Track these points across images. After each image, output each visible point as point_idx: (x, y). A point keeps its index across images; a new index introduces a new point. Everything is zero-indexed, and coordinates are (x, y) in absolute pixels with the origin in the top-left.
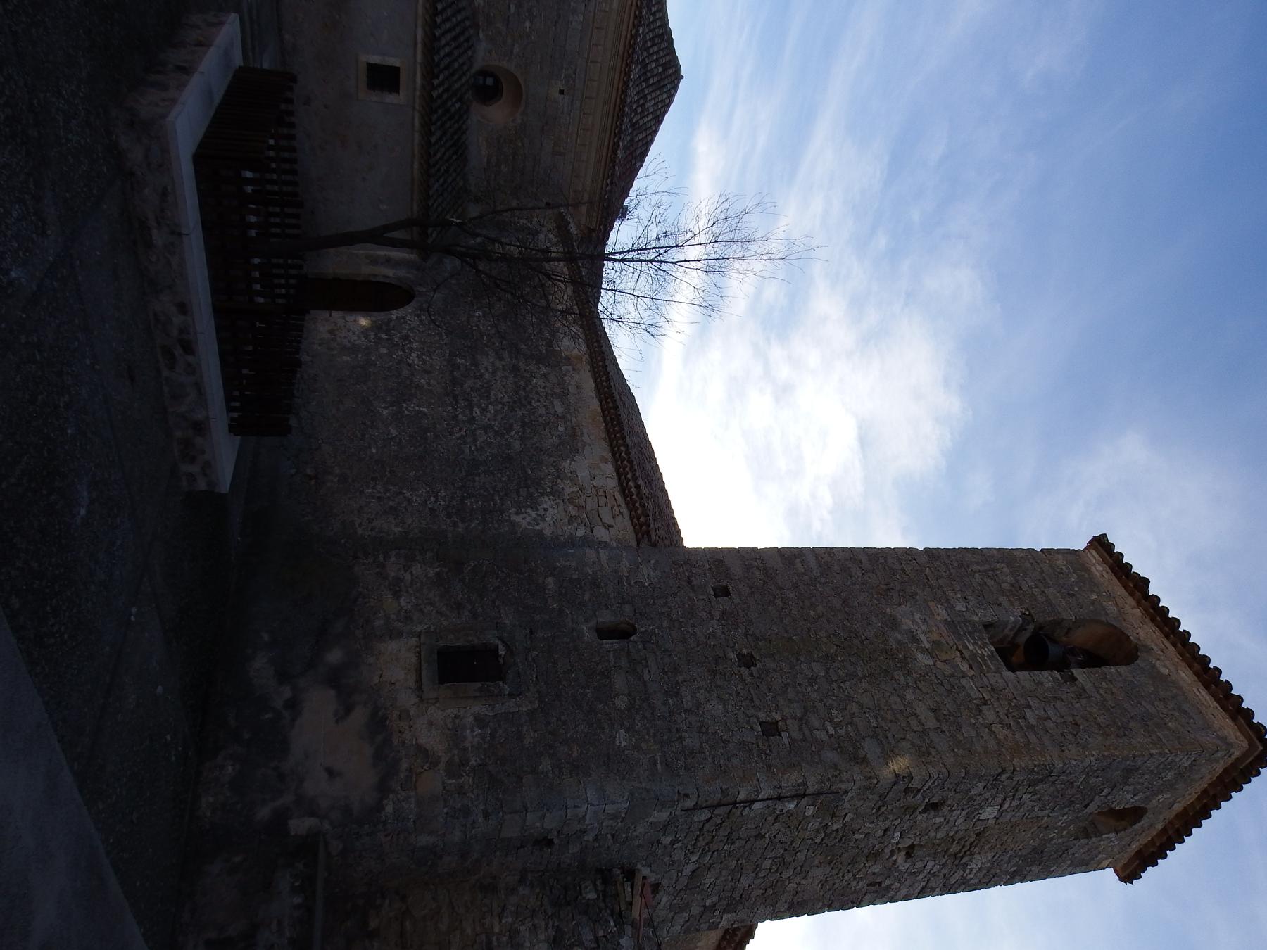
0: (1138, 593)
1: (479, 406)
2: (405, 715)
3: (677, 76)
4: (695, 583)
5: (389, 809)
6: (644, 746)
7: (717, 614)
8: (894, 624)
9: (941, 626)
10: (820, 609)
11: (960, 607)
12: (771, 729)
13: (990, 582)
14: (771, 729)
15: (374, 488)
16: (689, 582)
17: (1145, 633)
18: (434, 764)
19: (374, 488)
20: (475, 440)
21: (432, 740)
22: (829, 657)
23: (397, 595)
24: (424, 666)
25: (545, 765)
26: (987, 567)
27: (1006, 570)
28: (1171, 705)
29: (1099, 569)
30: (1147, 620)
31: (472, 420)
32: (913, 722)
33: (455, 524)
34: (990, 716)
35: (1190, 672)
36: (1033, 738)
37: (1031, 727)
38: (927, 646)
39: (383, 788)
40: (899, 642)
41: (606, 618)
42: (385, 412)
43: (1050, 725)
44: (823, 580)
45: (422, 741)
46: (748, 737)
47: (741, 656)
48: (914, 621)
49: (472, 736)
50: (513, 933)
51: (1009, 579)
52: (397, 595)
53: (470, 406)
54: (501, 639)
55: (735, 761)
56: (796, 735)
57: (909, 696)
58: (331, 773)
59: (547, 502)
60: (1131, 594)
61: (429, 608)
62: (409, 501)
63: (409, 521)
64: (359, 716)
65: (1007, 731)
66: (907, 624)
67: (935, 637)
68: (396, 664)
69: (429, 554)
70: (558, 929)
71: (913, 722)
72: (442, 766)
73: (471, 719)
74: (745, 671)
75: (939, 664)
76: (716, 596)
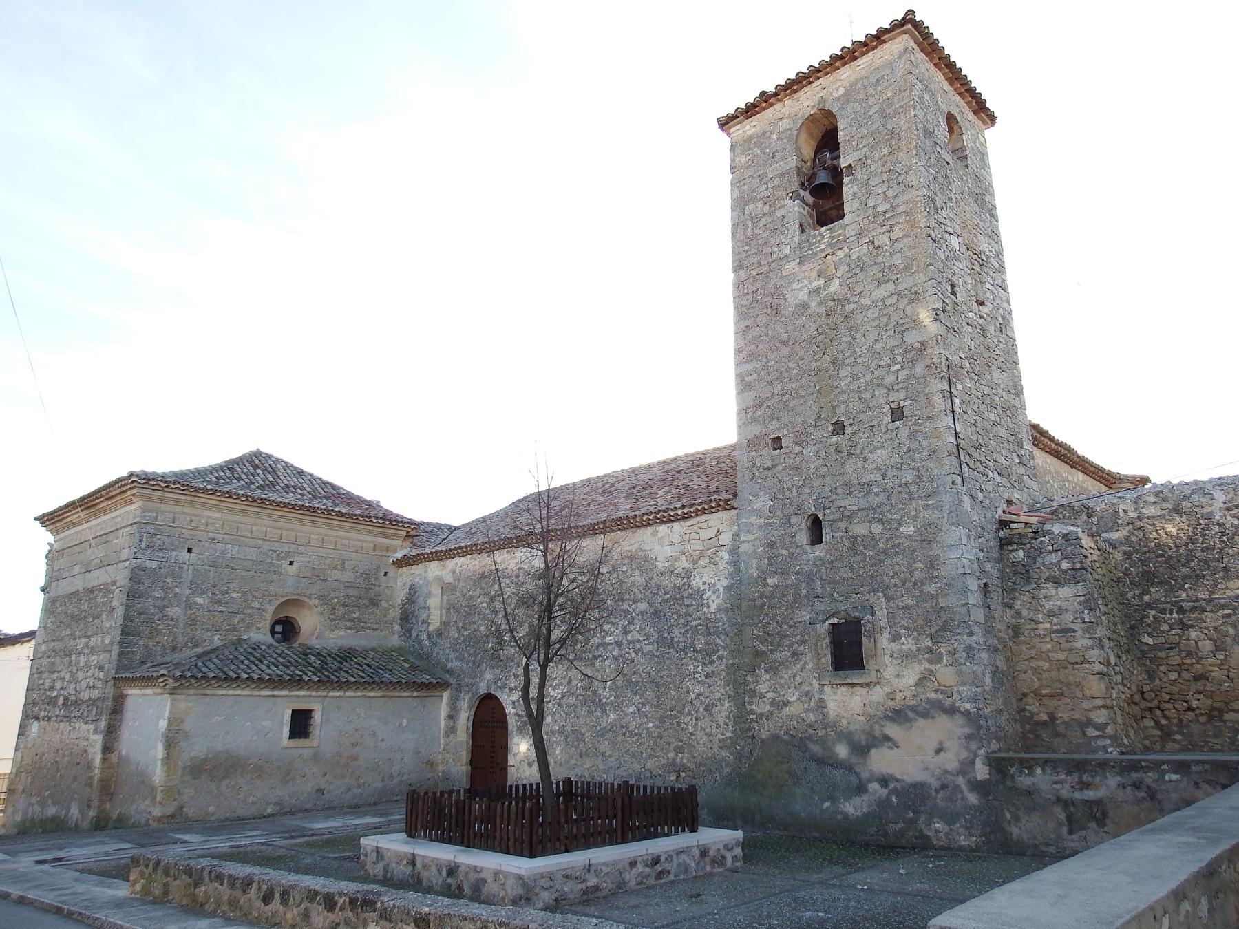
0: (772, 100)
1: (604, 637)
2: (891, 696)
3: (258, 454)
4: (769, 465)
5: (967, 706)
6: (913, 513)
7: (798, 449)
8: (804, 307)
9: (804, 268)
10: (791, 365)
11: (786, 250)
12: (897, 414)
13: (763, 222)
14: (897, 414)
15: (687, 724)
17: (806, 102)
18: (931, 673)
19: (687, 724)
20: (639, 641)
21: (911, 675)
23: (786, 704)
24: (849, 681)
25: (930, 589)
26: (749, 222)
27: (751, 206)
28: (871, 91)
29: (749, 128)
30: (795, 96)
31: (618, 644)
32: (889, 301)
33: (720, 658)
34: (882, 240)
35: (842, 70)
36: (902, 209)
37: (893, 208)
38: (822, 281)
39: (951, 711)
40: (820, 304)
41: (803, 537)
42: (612, 716)
43: (890, 193)
44: (764, 360)
45: (912, 683)
46: (904, 432)
47: (834, 432)
48: (800, 289)
49: (908, 644)
50: (1051, 614)
52: (786, 704)
53: (604, 645)
54: (824, 622)
55: (925, 444)
56: (902, 394)
57: (867, 302)
58: (939, 750)
59: (697, 582)
60: (772, 105)
61: (798, 678)
62: (699, 695)
63: (718, 695)
64: (892, 730)
65: (896, 228)
66: (803, 296)
67: (814, 274)
68: (847, 703)
69: (749, 678)
70: (1047, 580)
71: (889, 301)
72: (932, 667)
73: (893, 645)
74: (848, 430)
75: (839, 274)
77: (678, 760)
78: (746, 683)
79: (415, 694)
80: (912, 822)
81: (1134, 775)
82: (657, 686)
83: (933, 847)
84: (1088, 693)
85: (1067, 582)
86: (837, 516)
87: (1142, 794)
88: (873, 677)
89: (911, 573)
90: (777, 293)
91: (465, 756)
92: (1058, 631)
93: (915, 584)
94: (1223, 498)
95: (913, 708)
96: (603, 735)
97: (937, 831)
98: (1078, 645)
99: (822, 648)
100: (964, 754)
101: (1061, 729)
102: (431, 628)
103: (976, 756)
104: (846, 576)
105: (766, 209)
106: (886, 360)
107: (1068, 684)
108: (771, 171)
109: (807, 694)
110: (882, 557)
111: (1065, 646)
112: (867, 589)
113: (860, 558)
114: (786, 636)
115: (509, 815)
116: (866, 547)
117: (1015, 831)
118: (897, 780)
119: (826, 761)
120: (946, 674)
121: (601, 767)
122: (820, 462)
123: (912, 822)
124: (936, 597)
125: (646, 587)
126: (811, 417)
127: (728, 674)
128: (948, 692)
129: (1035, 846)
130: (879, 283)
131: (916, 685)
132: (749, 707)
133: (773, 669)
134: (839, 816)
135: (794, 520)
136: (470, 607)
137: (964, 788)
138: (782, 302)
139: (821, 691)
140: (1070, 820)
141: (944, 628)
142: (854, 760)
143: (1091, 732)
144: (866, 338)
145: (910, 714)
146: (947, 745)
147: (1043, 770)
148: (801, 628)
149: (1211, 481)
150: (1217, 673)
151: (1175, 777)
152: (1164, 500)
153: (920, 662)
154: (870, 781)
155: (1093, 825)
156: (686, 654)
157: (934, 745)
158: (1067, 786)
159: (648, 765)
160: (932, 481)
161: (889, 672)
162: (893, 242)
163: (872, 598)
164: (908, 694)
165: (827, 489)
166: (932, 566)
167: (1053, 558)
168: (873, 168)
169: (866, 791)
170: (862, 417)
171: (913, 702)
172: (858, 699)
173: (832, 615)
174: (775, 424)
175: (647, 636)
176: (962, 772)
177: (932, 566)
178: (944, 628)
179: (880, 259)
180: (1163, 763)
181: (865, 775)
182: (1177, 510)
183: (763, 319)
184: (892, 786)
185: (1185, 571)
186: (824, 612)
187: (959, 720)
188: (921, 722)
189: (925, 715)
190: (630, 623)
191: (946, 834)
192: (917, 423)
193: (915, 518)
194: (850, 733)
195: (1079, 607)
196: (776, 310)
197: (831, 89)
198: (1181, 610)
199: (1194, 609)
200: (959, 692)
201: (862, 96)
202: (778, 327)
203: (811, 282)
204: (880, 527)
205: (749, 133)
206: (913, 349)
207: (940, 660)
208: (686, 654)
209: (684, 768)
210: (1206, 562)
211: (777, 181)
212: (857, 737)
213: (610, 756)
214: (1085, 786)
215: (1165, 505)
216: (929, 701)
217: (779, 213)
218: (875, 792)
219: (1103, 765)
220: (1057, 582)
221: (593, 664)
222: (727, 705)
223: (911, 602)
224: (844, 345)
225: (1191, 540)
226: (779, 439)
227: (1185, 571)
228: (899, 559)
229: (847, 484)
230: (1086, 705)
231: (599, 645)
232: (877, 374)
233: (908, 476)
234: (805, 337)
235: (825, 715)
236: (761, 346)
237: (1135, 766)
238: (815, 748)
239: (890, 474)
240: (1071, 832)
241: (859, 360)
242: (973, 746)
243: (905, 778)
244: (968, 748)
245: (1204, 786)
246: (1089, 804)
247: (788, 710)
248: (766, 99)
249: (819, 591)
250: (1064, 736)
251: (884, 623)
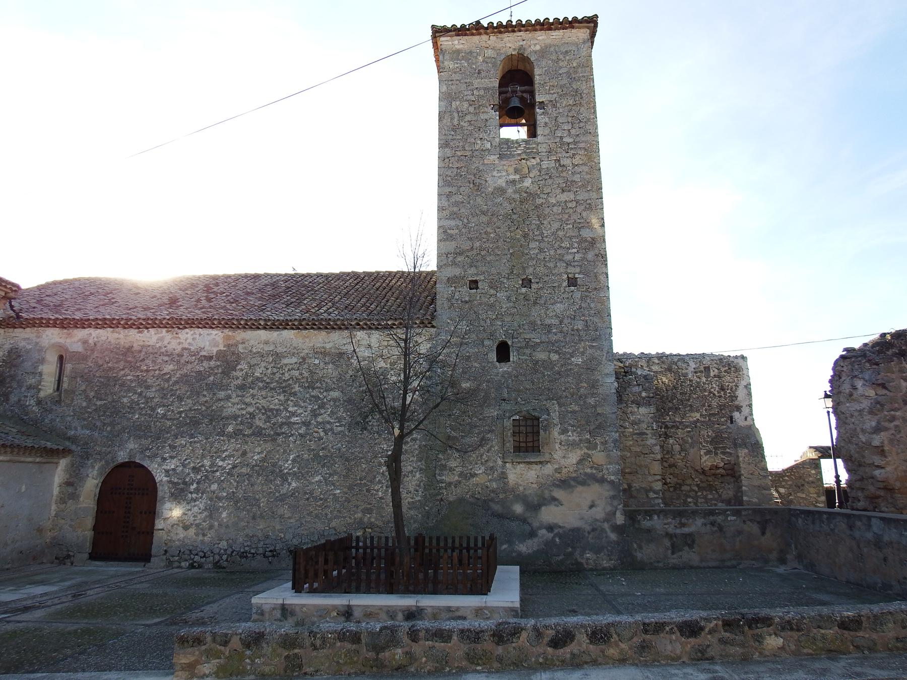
0: (482, 31)
1: (289, 417)
4: (467, 299)
5: (613, 478)
6: (582, 350)
7: (492, 292)
8: (501, 191)
9: (503, 163)
10: (489, 230)
11: (488, 146)
12: (572, 282)
13: (468, 118)
14: (572, 282)
15: (378, 491)
16: (466, 302)
17: (510, 43)
18: (589, 456)
19: (378, 491)
20: (329, 423)
21: (574, 457)
22: (525, 236)
23: (473, 475)
24: (528, 460)
25: (591, 401)
26: (456, 115)
27: (458, 103)
28: (561, 57)
29: (458, 43)
30: (500, 36)
31: (306, 424)
32: (569, 205)
33: (414, 440)
34: (566, 162)
35: (539, 33)
36: (582, 145)
37: (575, 143)
38: (518, 177)
39: (602, 481)
40: (515, 192)
41: (493, 356)
42: (294, 485)
43: (573, 132)
44: (465, 220)
45: (575, 462)
46: (577, 295)
47: (523, 286)
48: (500, 177)
49: (573, 437)
50: (634, 423)
51: (466, 105)
52: (473, 475)
53: (290, 424)
54: (509, 418)
55: (592, 305)
56: (578, 270)
57: (553, 201)
58: (591, 507)
60: (480, 34)
61: (484, 457)
64: (558, 494)
65: (578, 157)
66: (501, 182)
67: (511, 170)
68: (523, 476)
69: (440, 456)
70: (633, 402)
71: (569, 205)
72: (590, 452)
73: (562, 436)
74: (534, 286)
75: (532, 175)
76: (477, 288)
77: (366, 520)
78: (437, 460)
79: (38, 460)
80: (571, 554)
81: (712, 518)
82: (347, 460)
83: (585, 569)
84: (652, 472)
85: (644, 405)
86: (523, 344)
87: (716, 529)
88: (547, 457)
89: (578, 389)
90: (478, 173)
91: (90, 522)
92: (637, 434)
93: (581, 397)
94: (694, 366)
95: (574, 479)
96: (282, 500)
97: (588, 559)
98: (649, 443)
99: (507, 436)
100: (609, 509)
101: (635, 493)
102: (42, 394)
103: (617, 509)
104: (528, 387)
105: (471, 109)
106: (566, 244)
107: (640, 466)
108: (476, 83)
109: (492, 468)
110: (557, 376)
111: (640, 443)
112: (544, 397)
113: (540, 375)
114: (476, 426)
115: (123, 575)
116: (545, 368)
117: (639, 555)
118: (560, 527)
119: (506, 516)
120: (599, 457)
121: (278, 527)
122: (511, 304)
123: (571, 554)
124: (595, 407)
125: (340, 379)
126: (505, 271)
127: (420, 453)
128: (599, 468)
129: (651, 563)
130: (563, 191)
131: (578, 463)
132: (439, 478)
133: (464, 452)
134: (514, 554)
135: (487, 342)
136: (108, 378)
137: (608, 530)
138: (484, 183)
139: (504, 467)
140: (673, 546)
141: (599, 427)
142: (528, 514)
143: (652, 495)
144: (550, 227)
145: (572, 483)
146: (598, 502)
147: (658, 517)
148: (489, 422)
149: (687, 355)
150: (680, 464)
151: (733, 518)
152: (663, 362)
153: (581, 449)
154: (540, 528)
155: (686, 548)
156: (380, 435)
157: (588, 503)
158: (672, 526)
159: (333, 524)
160: (596, 330)
161: (558, 455)
162: (574, 166)
163: (548, 404)
164: (571, 469)
165: (516, 324)
166: (593, 386)
167: (636, 389)
168: (561, 110)
169: (536, 536)
170: (546, 279)
171: (574, 475)
172: (533, 472)
173: (516, 414)
174: (473, 270)
175: (339, 420)
176: (606, 520)
177: (593, 386)
178: (599, 427)
179: (564, 174)
180: (728, 510)
181: (536, 524)
182: (669, 369)
183: (466, 190)
184: (556, 531)
185: (670, 405)
186: (510, 411)
187: (607, 486)
188: (580, 488)
189: (583, 483)
190: (320, 407)
191: (594, 561)
192: (587, 291)
193: (583, 353)
194: (525, 496)
195: (651, 420)
196: (478, 187)
197: (536, 42)
198: (666, 427)
199: (673, 427)
200: (607, 469)
201: (554, 58)
202: (479, 200)
203: (508, 175)
204: (557, 357)
205: (458, 47)
206: (586, 241)
207: (595, 448)
208: (380, 435)
209: (372, 526)
210: (682, 401)
211: (482, 92)
212: (530, 499)
213: (289, 518)
214: (683, 525)
215: (663, 366)
216: (586, 474)
217: (483, 116)
218: (543, 536)
219: (694, 513)
220: (639, 405)
221: (274, 440)
222: (418, 475)
223: (577, 408)
224: (533, 226)
225: (675, 388)
226: (476, 282)
227: (670, 405)
228: (570, 379)
229: (533, 324)
230: (650, 479)
231: (283, 424)
232: (559, 252)
233: (580, 325)
234: (502, 212)
235: (506, 484)
236: (463, 210)
237: (712, 513)
238: (496, 507)
239: (566, 321)
240: (673, 553)
241: (546, 240)
242: (615, 503)
243: (566, 525)
244: (611, 505)
245: (748, 523)
246: (685, 536)
247: (475, 480)
248: (477, 28)
249: (506, 395)
250: (635, 497)
251: (556, 421)
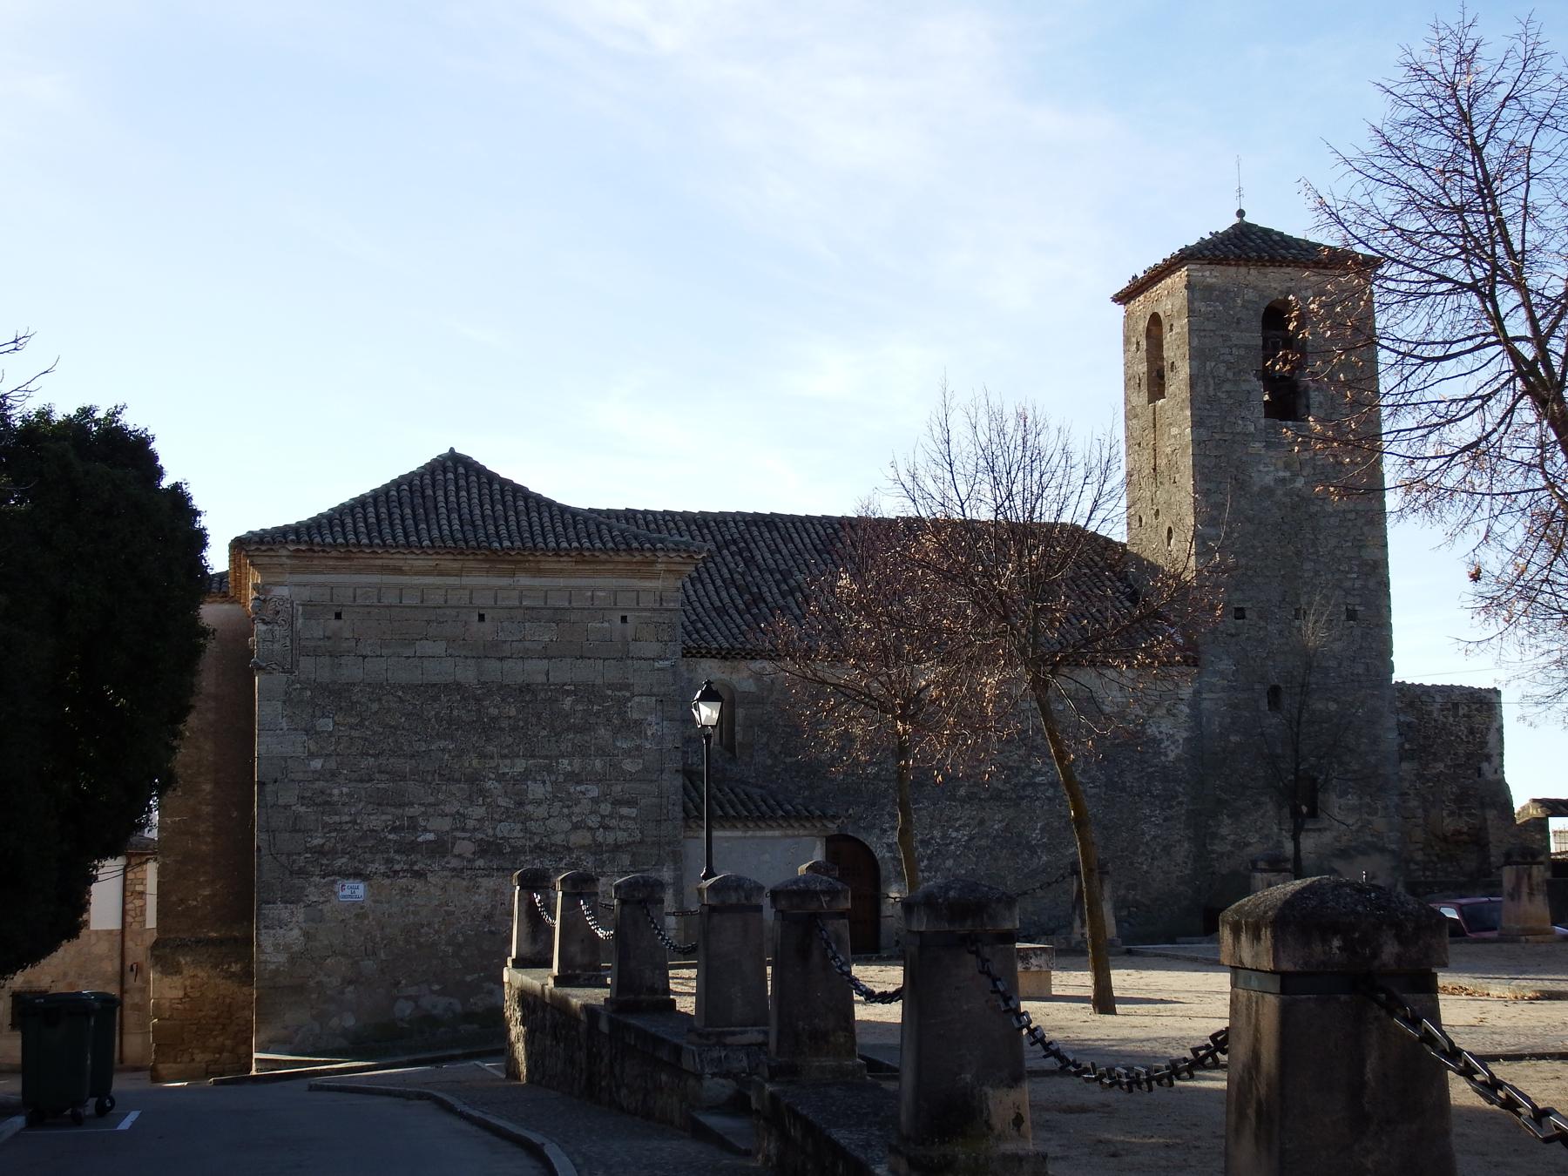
2: (1337, 839)
5: (1394, 846)
7: (1262, 623)
8: (1268, 492)
10: (1256, 543)
13: (1227, 387)
14: (1352, 615)
16: (1232, 636)
18: (1370, 822)
22: (1298, 553)
23: (1248, 844)
33: (1181, 803)
40: (1285, 495)
41: (1264, 704)
46: (1357, 632)
51: (1223, 368)
52: (1248, 844)
53: (1034, 785)
59: (1152, 730)
62: (1155, 837)
63: (1177, 837)
66: (1269, 480)
67: (1280, 464)
76: (1244, 617)
105: (1230, 375)
109: (1267, 837)
120: (1379, 823)
135: (1257, 686)
174: (1237, 595)
211: (1242, 352)
217: (1245, 387)
226: (1242, 609)
231: (1025, 786)
247: (1250, 850)
